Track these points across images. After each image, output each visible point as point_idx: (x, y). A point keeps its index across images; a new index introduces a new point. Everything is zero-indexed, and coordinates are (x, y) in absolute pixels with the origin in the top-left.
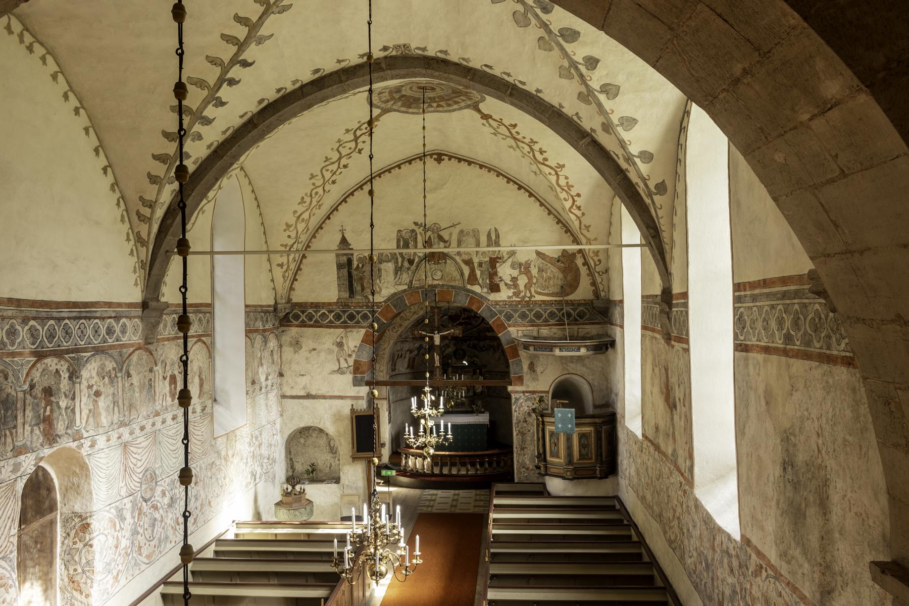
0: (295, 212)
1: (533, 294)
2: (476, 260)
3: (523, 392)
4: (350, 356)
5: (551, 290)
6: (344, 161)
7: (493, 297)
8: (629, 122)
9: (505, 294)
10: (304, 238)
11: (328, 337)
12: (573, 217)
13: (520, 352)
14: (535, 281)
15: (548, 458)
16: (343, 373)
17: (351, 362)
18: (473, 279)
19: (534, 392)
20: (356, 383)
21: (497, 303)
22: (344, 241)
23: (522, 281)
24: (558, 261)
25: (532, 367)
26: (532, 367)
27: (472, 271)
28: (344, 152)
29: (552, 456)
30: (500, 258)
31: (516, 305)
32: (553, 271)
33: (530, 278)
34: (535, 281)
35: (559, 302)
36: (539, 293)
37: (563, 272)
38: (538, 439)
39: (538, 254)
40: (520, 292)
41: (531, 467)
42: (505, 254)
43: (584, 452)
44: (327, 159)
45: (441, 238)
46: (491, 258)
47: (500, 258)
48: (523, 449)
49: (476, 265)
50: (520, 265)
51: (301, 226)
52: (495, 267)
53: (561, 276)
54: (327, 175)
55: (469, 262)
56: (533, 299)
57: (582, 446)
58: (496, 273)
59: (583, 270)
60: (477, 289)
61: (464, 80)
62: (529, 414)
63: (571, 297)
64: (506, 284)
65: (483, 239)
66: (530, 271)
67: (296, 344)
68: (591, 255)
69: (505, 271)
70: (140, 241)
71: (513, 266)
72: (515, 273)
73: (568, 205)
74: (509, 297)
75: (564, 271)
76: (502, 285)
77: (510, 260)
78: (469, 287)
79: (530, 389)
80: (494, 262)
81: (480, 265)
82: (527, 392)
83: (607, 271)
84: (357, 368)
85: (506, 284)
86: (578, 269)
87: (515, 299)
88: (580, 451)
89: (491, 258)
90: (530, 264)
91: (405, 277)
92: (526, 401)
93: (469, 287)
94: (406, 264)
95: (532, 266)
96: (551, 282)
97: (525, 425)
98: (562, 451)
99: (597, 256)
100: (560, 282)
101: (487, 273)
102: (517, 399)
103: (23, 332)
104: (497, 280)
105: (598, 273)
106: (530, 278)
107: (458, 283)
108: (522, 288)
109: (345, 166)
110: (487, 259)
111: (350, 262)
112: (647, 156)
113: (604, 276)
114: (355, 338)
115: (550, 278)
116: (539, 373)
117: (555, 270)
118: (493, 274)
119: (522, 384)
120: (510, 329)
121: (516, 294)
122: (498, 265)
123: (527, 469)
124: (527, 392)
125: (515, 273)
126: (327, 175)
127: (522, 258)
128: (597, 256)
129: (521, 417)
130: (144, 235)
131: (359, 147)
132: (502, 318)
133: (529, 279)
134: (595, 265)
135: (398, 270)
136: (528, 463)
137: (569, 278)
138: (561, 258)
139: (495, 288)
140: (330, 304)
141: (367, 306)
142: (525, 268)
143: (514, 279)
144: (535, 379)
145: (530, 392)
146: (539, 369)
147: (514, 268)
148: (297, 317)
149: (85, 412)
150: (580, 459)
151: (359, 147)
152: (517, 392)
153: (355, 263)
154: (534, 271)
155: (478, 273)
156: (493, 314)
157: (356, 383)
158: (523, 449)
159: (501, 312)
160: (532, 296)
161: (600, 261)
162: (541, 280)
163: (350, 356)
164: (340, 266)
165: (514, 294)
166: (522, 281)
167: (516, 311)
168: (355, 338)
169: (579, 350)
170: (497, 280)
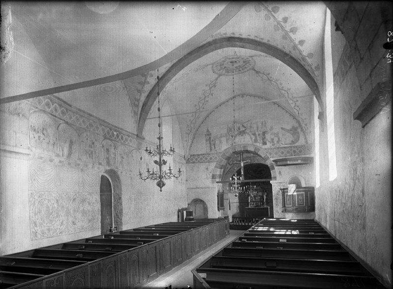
0: (190, 120)
2: (257, 133)
4: (211, 172)
6: (207, 99)
8: (302, 42)
9: (269, 145)
10: (194, 131)
11: (203, 166)
12: (295, 111)
16: (208, 179)
17: (211, 175)
18: (256, 141)
20: (213, 182)
22: (208, 131)
23: (276, 139)
27: (256, 137)
28: (207, 95)
33: (279, 139)
35: (291, 147)
39: (282, 128)
40: (275, 144)
44: (200, 98)
45: (243, 126)
49: (257, 135)
51: (192, 126)
54: (201, 105)
55: (254, 134)
60: (258, 144)
61: (241, 44)
63: (297, 144)
65: (260, 125)
67: (192, 170)
68: (304, 125)
69: (268, 137)
70: (136, 114)
72: (273, 137)
73: (293, 106)
76: (267, 142)
78: (255, 144)
80: (264, 133)
81: (259, 135)
84: (214, 177)
86: (298, 133)
91: (230, 142)
93: (255, 144)
94: (231, 137)
100: (291, 139)
103: (100, 128)
106: (279, 139)
107: (250, 142)
109: (207, 101)
110: (261, 132)
111: (210, 138)
112: (311, 55)
114: (212, 166)
118: (264, 139)
121: (273, 145)
125: (273, 137)
126: (201, 105)
127: (275, 131)
130: (136, 110)
131: (212, 93)
135: (227, 140)
139: (265, 143)
140: (203, 154)
141: (216, 154)
142: (277, 135)
143: (273, 139)
148: (192, 160)
149: (119, 161)
151: (212, 93)
153: (212, 139)
154: (280, 135)
155: (258, 138)
157: (213, 182)
163: (211, 172)
164: (207, 141)
166: (276, 139)
168: (212, 166)
170: (265, 140)
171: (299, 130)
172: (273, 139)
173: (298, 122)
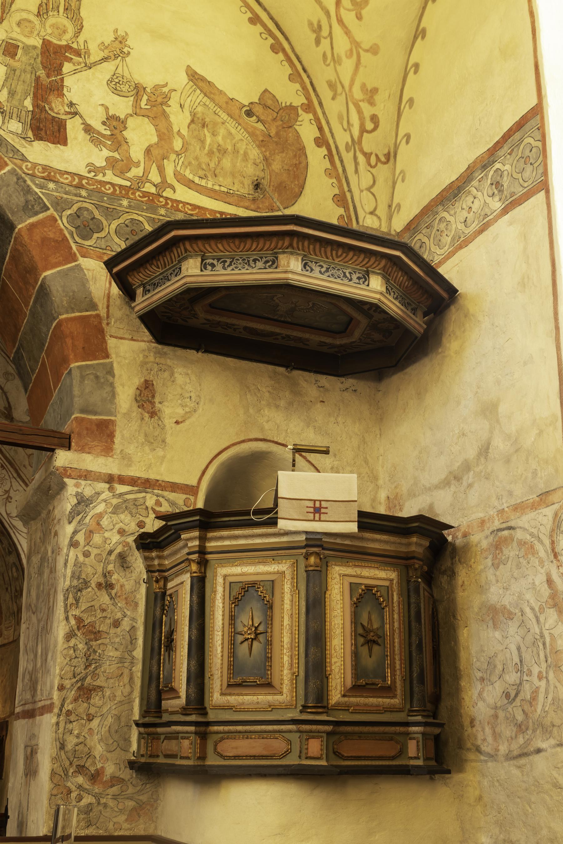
1: (171, 179)
3: (110, 479)
5: (225, 183)
7: (39, 153)
13: (111, 343)
14: (178, 144)
15: (216, 696)
19: (147, 484)
21: (50, 174)
24: (249, 113)
25: (146, 396)
26: (146, 396)
29: (235, 684)
30: (78, 53)
31: (113, 197)
32: (232, 134)
33: (165, 135)
34: (178, 144)
36: (189, 184)
37: (262, 144)
38: (159, 641)
39: (194, 77)
41: (110, 769)
42: (93, 47)
43: (369, 662)
46: (46, 44)
47: (78, 53)
48: (86, 692)
50: (138, 90)
52: (59, 70)
53: (254, 153)
56: (168, 193)
57: (366, 637)
58: (58, 89)
59: (316, 158)
62: (122, 558)
64: (88, 129)
66: (165, 115)
68: (357, 94)
71: (115, 84)
72: (122, 107)
74: (92, 168)
75: (263, 143)
76: (73, 128)
77: (108, 68)
79: (134, 472)
80: (54, 57)
82: (122, 480)
83: (390, 157)
85: (88, 129)
86: (302, 149)
87: (109, 177)
88: (356, 655)
89: (46, 44)
90: (167, 98)
92: (116, 510)
95: (174, 102)
96: (227, 163)
97: (105, 599)
98: (287, 663)
99: (372, 103)
100: (250, 170)
101: (28, 78)
102: (83, 502)
104: (58, 108)
105: (368, 156)
106: (165, 135)
108: (137, 152)
113: (382, 171)
115: (223, 151)
116: (168, 422)
117: (239, 134)
118: (47, 89)
119: (108, 450)
120: (84, 262)
122: (67, 67)
123: (95, 777)
124: (122, 480)
125: (122, 107)
128: (372, 103)
129: (93, 571)
132: (63, 223)
133: (161, 136)
134: (363, 130)
136: (99, 750)
137: (276, 166)
138: (258, 110)
143: (116, 123)
144: (156, 441)
145: (132, 481)
146: (170, 410)
147: (116, 91)
150: (357, 688)
152: (86, 475)
154: (179, 120)
156: (33, 205)
158: (86, 692)
159: (60, 205)
160: (164, 184)
161: (374, 119)
162: (195, 146)
165: (111, 163)
166: (140, 135)
167: (110, 214)
169: (365, 277)
171: (307, 131)
172: (116, 123)
173: (299, 73)
